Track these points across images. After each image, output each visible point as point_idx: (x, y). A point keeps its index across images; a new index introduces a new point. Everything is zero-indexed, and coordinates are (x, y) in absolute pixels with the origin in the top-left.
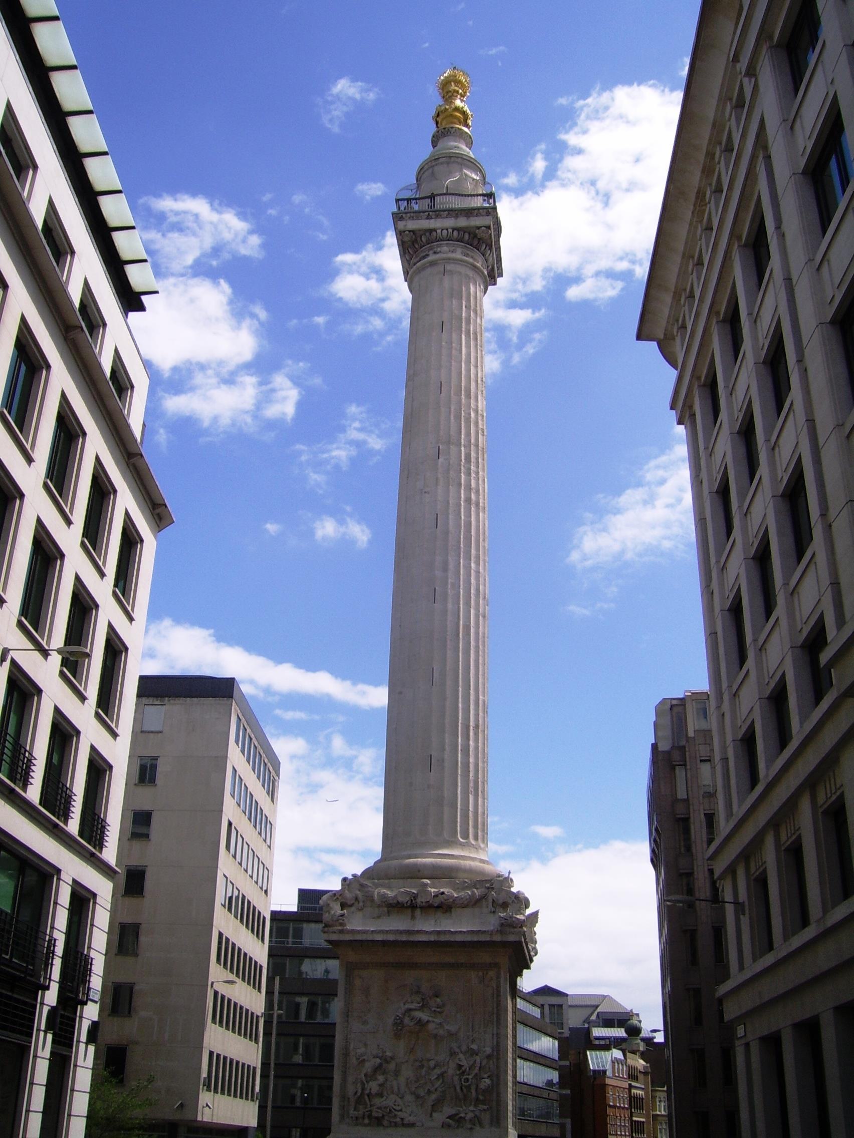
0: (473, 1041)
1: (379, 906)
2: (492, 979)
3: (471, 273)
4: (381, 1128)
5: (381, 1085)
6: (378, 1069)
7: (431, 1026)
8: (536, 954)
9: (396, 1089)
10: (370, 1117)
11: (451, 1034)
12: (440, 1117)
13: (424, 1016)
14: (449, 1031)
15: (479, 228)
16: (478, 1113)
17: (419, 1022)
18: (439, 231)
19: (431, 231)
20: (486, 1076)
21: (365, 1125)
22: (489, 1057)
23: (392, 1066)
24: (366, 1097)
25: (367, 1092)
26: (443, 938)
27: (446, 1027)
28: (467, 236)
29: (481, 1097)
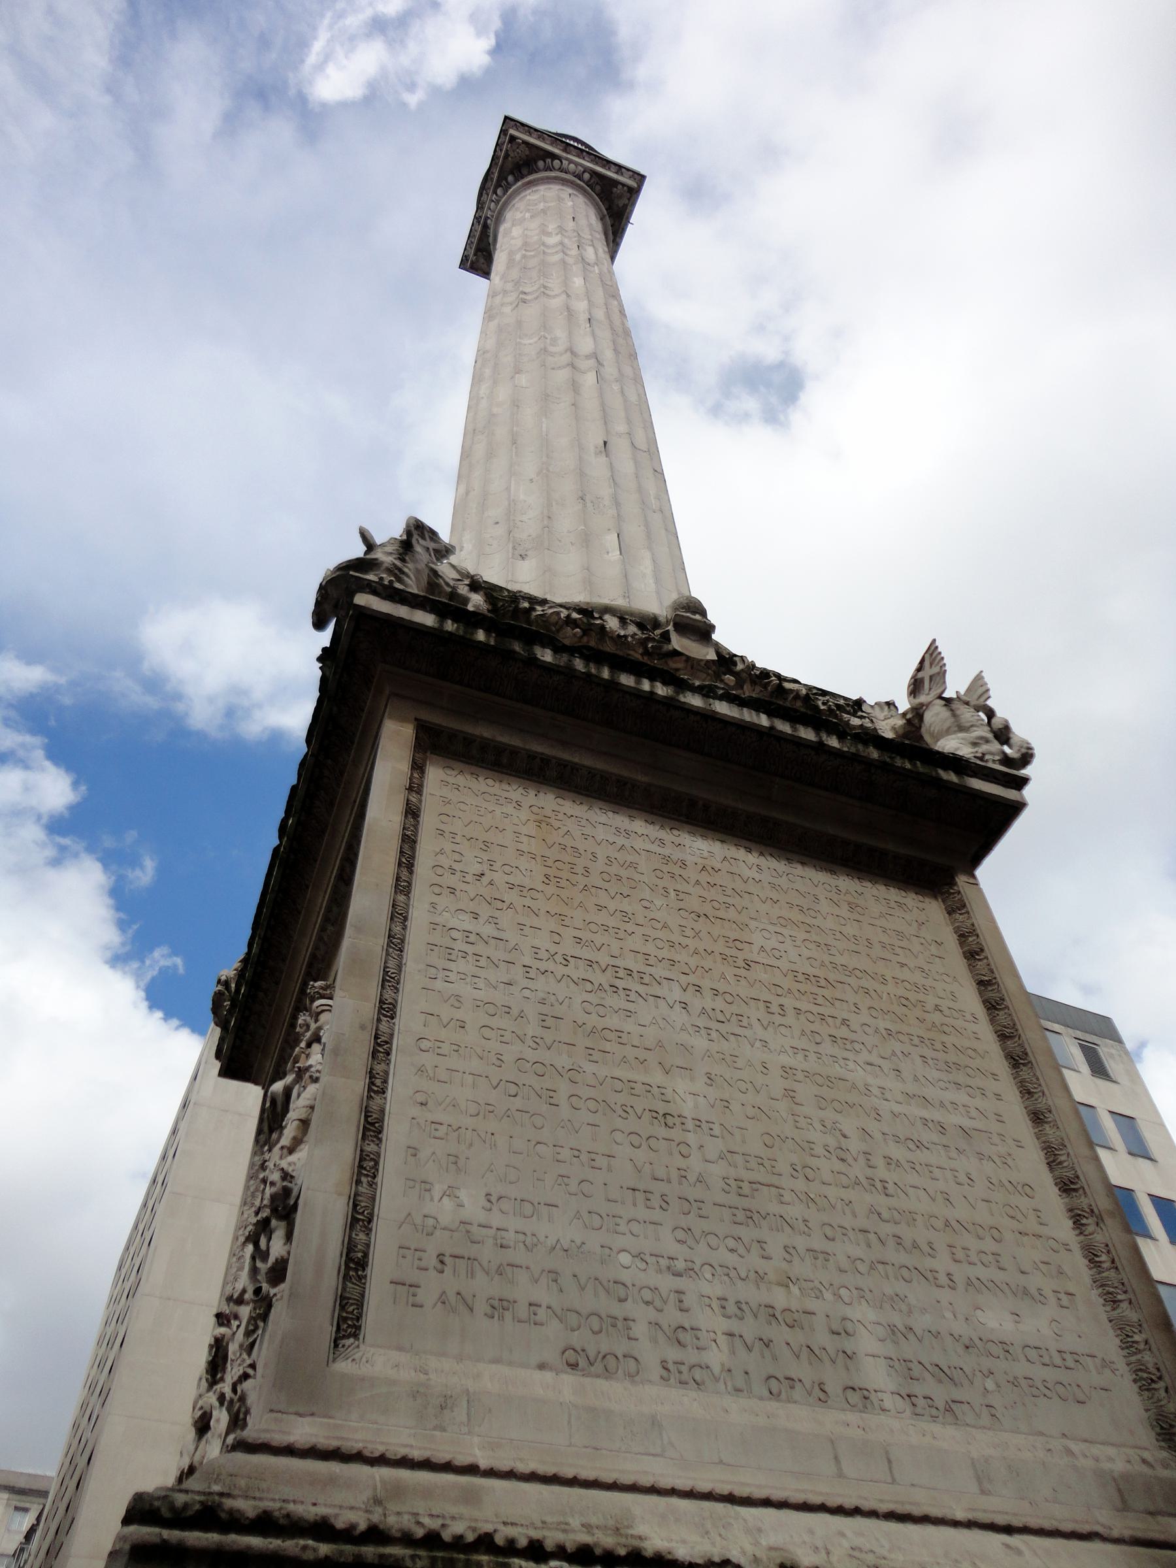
8: (1026, 758)
28: (510, 178)
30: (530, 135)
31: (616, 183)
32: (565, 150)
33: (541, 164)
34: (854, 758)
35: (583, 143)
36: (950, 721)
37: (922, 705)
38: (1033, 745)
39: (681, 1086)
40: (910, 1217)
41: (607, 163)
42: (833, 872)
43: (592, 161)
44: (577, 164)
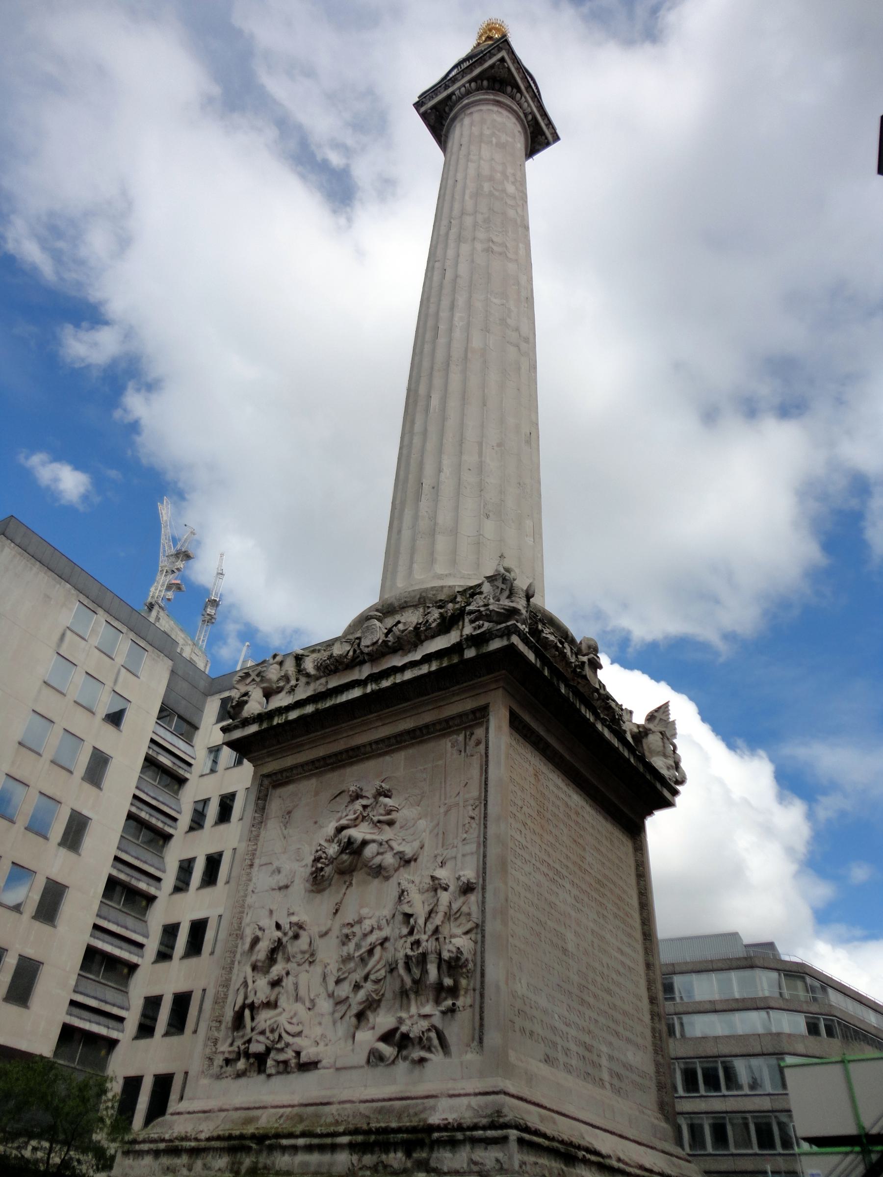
0: (443, 864)
1: (317, 678)
2: (478, 743)
3: (495, 108)
4: (263, 1077)
5: (276, 983)
6: (277, 948)
7: (369, 851)
8: (681, 782)
9: (302, 992)
10: (247, 1055)
11: (406, 861)
12: (367, 1037)
13: (358, 833)
14: (400, 855)
15: (492, 67)
16: (437, 1020)
17: (350, 841)
18: (457, 92)
19: (449, 97)
20: (459, 931)
21: (240, 1075)
22: (467, 889)
23: (303, 943)
24: (247, 1013)
25: (249, 1001)
26: (385, 684)
27: (397, 848)
28: (485, 83)
29: (448, 982)
30: (513, 63)
31: (543, 134)
32: (526, 89)
33: (509, 89)
34: (635, 769)
35: (539, 94)
36: (661, 749)
37: (650, 730)
38: (688, 777)
39: (570, 936)
40: (614, 1007)
41: (545, 115)
42: (606, 819)
43: (537, 107)
44: (529, 105)
